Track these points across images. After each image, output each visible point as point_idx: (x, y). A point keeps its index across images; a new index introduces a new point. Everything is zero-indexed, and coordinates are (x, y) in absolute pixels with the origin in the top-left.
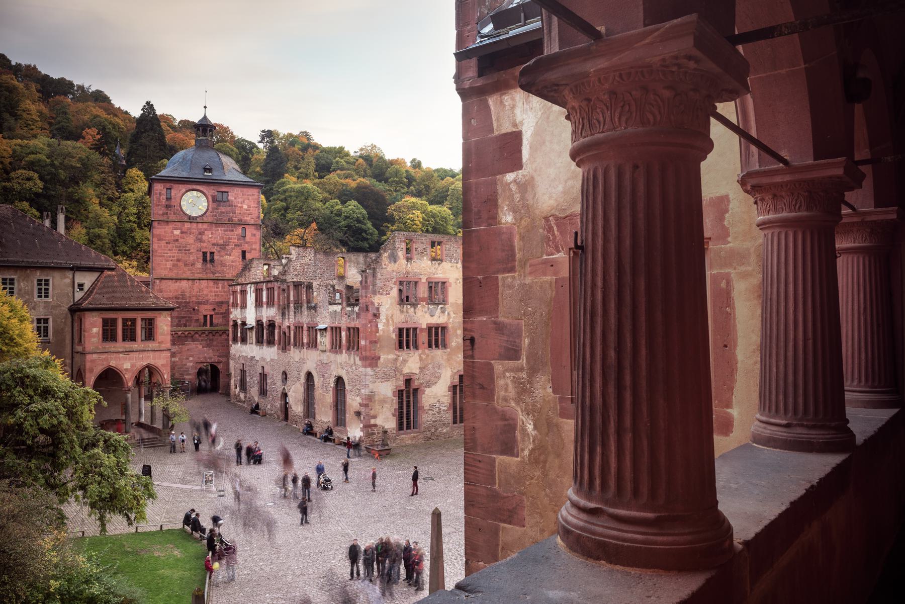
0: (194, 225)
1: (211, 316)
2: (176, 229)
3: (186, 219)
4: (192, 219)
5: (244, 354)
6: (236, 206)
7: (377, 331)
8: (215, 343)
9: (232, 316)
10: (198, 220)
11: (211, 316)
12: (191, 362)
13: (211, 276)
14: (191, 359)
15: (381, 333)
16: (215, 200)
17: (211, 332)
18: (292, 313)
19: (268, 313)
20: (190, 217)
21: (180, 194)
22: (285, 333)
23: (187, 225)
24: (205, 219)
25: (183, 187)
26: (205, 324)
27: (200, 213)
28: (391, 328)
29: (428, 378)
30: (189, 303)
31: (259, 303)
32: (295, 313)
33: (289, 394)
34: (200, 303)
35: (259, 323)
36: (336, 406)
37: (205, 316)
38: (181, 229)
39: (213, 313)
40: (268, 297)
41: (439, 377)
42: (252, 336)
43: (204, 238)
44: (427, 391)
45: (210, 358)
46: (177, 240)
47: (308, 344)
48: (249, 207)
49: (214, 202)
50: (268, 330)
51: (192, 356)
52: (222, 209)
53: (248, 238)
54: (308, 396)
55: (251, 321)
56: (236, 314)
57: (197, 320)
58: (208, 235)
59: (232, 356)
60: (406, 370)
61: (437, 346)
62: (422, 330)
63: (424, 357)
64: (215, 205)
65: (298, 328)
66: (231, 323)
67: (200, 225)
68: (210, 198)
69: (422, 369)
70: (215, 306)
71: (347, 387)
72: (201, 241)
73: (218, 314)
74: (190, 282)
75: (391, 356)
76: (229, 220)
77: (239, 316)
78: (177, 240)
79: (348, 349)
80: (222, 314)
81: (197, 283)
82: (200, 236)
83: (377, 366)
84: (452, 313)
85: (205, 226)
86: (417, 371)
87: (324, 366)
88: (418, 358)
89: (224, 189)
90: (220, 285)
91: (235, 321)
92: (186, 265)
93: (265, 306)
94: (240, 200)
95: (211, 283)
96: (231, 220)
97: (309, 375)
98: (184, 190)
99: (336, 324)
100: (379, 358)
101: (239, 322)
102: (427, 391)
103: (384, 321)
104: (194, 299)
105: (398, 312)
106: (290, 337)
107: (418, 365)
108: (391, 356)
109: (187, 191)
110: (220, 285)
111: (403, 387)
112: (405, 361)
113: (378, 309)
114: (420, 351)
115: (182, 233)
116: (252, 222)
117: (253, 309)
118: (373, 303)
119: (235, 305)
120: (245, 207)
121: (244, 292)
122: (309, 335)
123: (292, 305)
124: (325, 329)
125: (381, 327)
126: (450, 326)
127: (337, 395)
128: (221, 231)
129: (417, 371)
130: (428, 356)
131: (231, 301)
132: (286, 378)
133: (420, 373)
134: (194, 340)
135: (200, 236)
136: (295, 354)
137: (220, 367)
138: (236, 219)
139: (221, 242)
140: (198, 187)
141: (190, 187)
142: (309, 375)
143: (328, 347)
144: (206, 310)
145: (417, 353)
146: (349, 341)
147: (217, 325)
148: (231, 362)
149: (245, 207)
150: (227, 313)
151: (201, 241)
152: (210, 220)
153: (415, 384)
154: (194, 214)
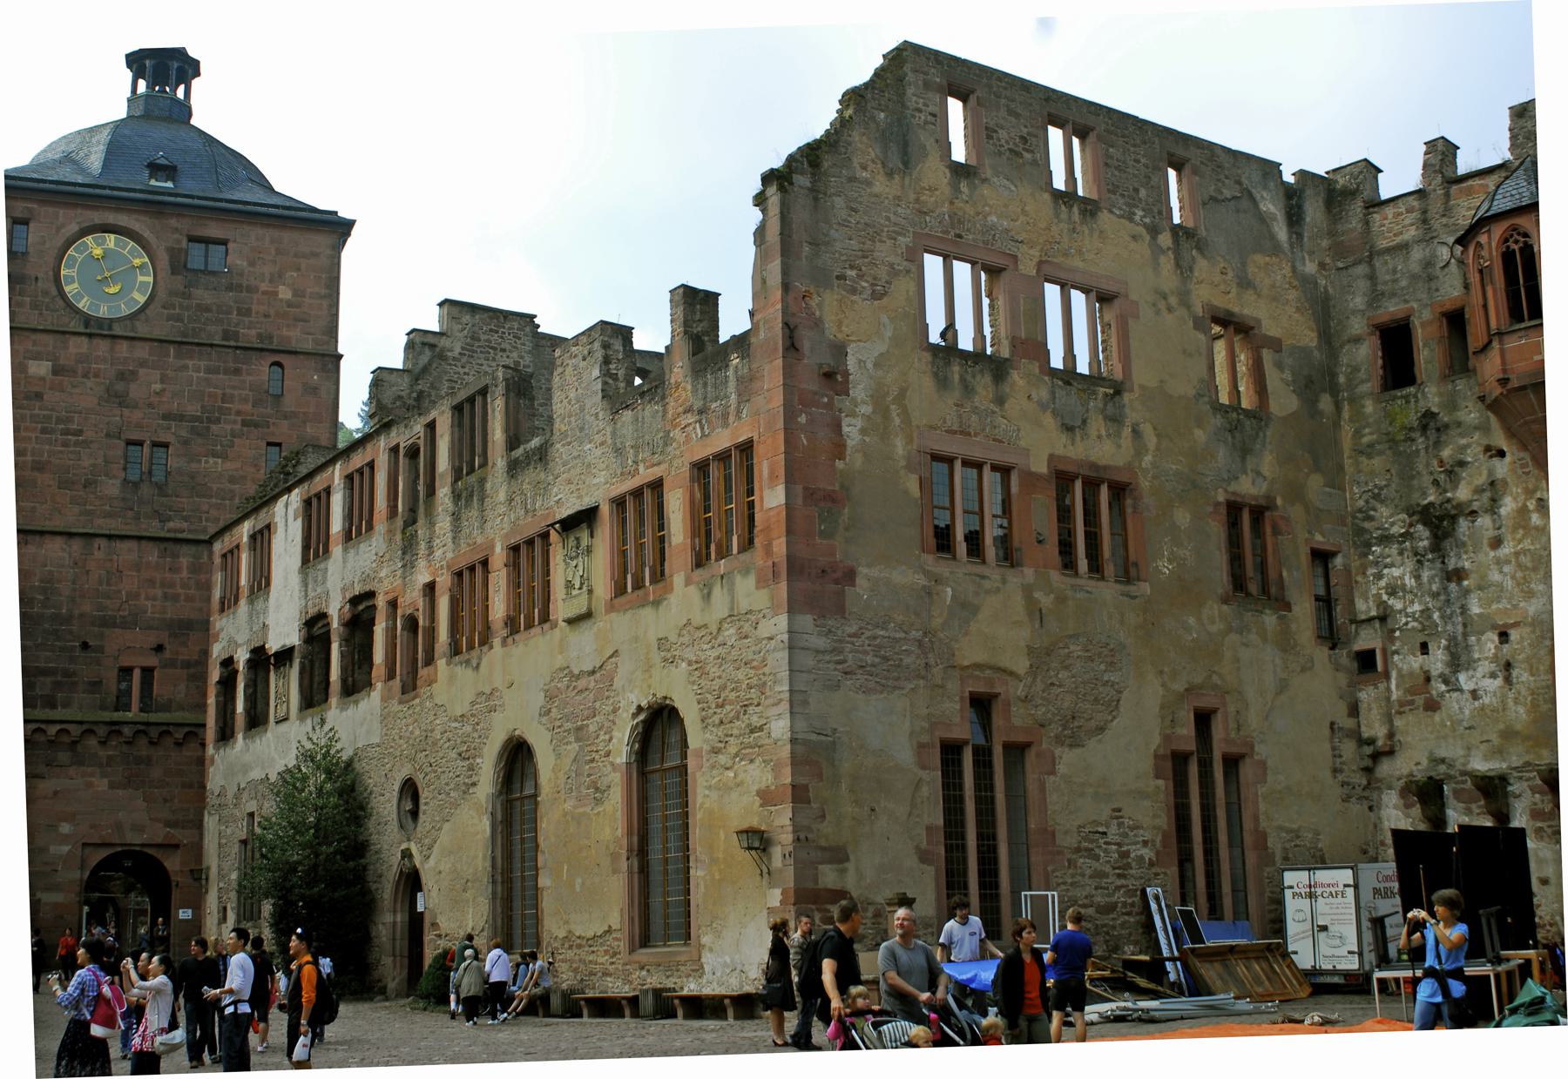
0: (103, 346)
1: (148, 672)
2: (37, 357)
3: (75, 325)
4: (95, 329)
5: (256, 774)
6: (250, 289)
7: (839, 449)
8: (156, 773)
9: (217, 651)
10: (117, 330)
11: (148, 672)
12: (65, 839)
13: (153, 528)
14: (65, 828)
15: (854, 460)
16: (178, 264)
17: (142, 730)
18: (444, 524)
19: (344, 572)
20: (88, 320)
21: (59, 242)
22: (412, 623)
23: (77, 346)
24: (142, 329)
25: (72, 220)
26: (122, 703)
27: (125, 310)
28: (900, 447)
29: (1068, 702)
30: (68, 619)
31: (314, 548)
32: (456, 517)
33: (427, 879)
34: (107, 622)
35: (315, 625)
36: (641, 850)
37: (126, 672)
38: (55, 359)
39: (152, 661)
40: (349, 516)
41: (1114, 706)
42: (286, 687)
43: (135, 391)
44: (1067, 759)
45: (140, 829)
46: (39, 396)
47: (512, 625)
48: (297, 293)
49: (175, 270)
50: (346, 641)
51: (70, 818)
52: (203, 295)
53: (289, 403)
54: (508, 855)
55: (284, 632)
56: (232, 637)
57: (95, 686)
58: (149, 383)
59: (211, 800)
60: (971, 652)
61: (1096, 567)
62: (1030, 478)
63: (1045, 600)
64: (178, 282)
65: (471, 575)
66: (215, 675)
67: (123, 348)
68: (164, 259)
69: (1041, 657)
70: (164, 637)
71: (694, 741)
72: (122, 400)
73: (171, 664)
74: (77, 545)
75: (905, 577)
76: (226, 335)
77: (241, 638)
78: (39, 396)
79: (700, 561)
80: (187, 665)
81: (100, 549)
82: (120, 387)
83: (840, 610)
84: (1147, 429)
85: (142, 351)
86: (1021, 665)
87: (574, 692)
88: (1018, 600)
89: (213, 230)
90: (184, 561)
91: (228, 663)
92: (64, 484)
93: (337, 550)
94: (267, 270)
95: (152, 554)
96: (236, 336)
97: (517, 755)
98: (74, 228)
99: (645, 475)
100: (850, 576)
101: (242, 657)
102: (1067, 759)
103: (866, 409)
104: (87, 608)
105: (928, 382)
106: (431, 632)
107: (1023, 635)
108: (905, 577)
109: (85, 232)
110: (184, 561)
111: (962, 728)
112: (966, 609)
113: (840, 350)
114: (1029, 573)
115: (56, 371)
116: (309, 346)
117: (295, 579)
118: (817, 324)
119: (229, 602)
120: (285, 293)
121: (262, 538)
122: (515, 584)
123: (443, 492)
124: (587, 517)
125: (852, 430)
126: (1144, 484)
127: (644, 799)
128: (195, 369)
129: (1021, 665)
130: (1061, 600)
131: (217, 594)
132: (415, 814)
133: (1034, 671)
134: (79, 761)
135: (120, 387)
136: (450, 685)
137: (172, 863)
138: (249, 335)
139: (193, 409)
140: (123, 220)
141: (98, 217)
142: (517, 755)
143: (602, 586)
144: (130, 647)
145: (1015, 579)
146: (702, 530)
147: (166, 707)
148: (210, 822)
149: (285, 293)
150: (201, 628)
151: (122, 400)
152: (158, 333)
153: (1011, 722)
154: (103, 312)
